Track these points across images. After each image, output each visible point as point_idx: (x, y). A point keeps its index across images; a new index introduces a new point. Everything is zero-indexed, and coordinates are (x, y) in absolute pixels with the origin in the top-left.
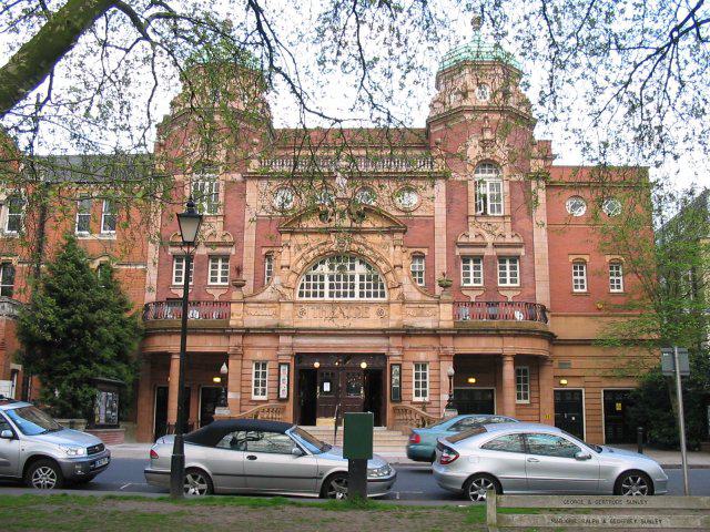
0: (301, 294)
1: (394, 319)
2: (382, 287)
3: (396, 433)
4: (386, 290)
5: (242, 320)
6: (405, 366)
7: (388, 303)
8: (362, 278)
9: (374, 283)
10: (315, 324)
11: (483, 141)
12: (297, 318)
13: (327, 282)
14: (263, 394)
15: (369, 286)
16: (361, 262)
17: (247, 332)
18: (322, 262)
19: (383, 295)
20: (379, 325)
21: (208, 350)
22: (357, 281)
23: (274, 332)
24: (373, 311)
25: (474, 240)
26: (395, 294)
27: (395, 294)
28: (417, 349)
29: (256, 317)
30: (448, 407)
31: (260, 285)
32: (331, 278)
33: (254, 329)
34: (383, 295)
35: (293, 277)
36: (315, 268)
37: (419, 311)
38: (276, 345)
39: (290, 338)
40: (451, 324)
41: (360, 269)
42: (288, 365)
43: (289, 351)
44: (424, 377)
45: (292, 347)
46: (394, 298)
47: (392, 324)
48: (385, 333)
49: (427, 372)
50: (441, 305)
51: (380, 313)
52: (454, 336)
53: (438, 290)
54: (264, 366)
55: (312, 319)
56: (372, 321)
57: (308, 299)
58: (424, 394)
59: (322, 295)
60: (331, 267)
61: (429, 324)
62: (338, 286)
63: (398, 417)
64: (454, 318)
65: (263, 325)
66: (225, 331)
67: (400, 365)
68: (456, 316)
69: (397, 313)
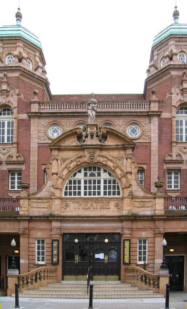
0: (66, 194)
1: (127, 209)
2: (118, 188)
3: (127, 285)
4: (121, 190)
5: (28, 211)
6: (133, 241)
7: (123, 199)
8: (105, 182)
9: (113, 186)
10: (75, 213)
11: (182, 90)
12: (63, 210)
13: (82, 185)
14: (43, 260)
15: (110, 187)
16: (105, 171)
17: (31, 219)
18: (80, 171)
19: (119, 194)
20: (116, 213)
21: (7, 231)
22: (102, 185)
23: (49, 218)
24: (112, 204)
25: (175, 159)
26: (127, 192)
27: (127, 192)
28: (140, 229)
29: (37, 209)
30: (162, 267)
31: (40, 185)
32: (85, 182)
33: (36, 217)
34: (119, 194)
35: (60, 180)
36: (75, 175)
37: (142, 204)
38: (50, 228)
39: (59, 223)
40: (163, 212)
41: (104, 176)
42: (58, 241)
43: (58, 232)
44: (145, 248)
45: (60, 228)
46: (126, 195)
47: (125, 213)
48: (121, 219)
49: (147, 245)
50: (157, 200)
51: (117, 206)
52: (164, 220)
53: (154, 189)
54: (43, 242)
55: (73, 210)
56: (112, 211)
57: (70, 196)
58: (144, 259)
59: (79, 193)
60: (86, 175)
61: (148, 212)
62: (90, 188)
63: (128, 275)
64: (165, 208)
65: (41, 214)
66: (16, 218)
67: (130, 240)
68: (166, 208)
69: (128, 206)
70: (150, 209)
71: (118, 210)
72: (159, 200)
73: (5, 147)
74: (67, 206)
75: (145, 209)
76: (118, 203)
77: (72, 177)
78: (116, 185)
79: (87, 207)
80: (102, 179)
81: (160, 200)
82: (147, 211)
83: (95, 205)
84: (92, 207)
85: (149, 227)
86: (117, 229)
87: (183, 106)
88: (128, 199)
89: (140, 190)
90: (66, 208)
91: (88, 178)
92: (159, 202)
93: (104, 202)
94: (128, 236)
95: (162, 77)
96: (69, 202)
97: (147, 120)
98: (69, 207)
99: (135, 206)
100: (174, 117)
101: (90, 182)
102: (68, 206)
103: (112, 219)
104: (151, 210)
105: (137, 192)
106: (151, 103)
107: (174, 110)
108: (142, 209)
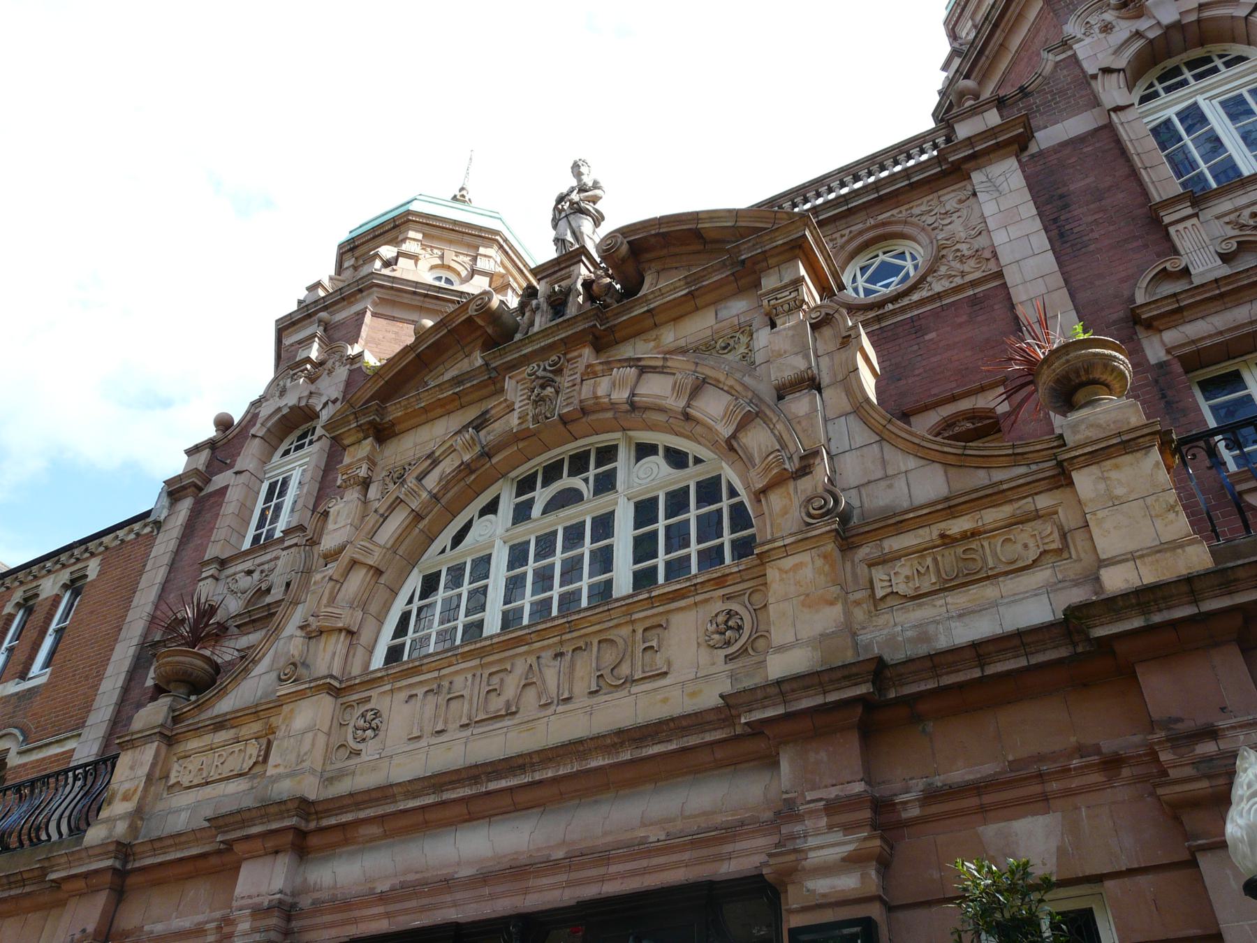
8: (645, 511)
32: (518, 556)
37: (948, 559)
60: (522, 513)
69: (810, 602)
70: (1041, 576)
71: (730, 666)
72: (1114, 475)
73: (258, 561)
74: (369, 733)
75: (989, 592)
76: (730, 614)
77: (443, 551)
78: (725, 504)
79: (497, 704)
80: (622, 501)
81: (1117, 467)
82: (1017, 598)
83: (551, 675)
84: (531, 695)
85: (1080, 751)
86: (731, 832)
87: (1170, 63)
88: (805, 557)
89: (912, 463)
90: (360, 746)
91: (539, 522)
92: (1119, 491)
93: (625, 631)
94: (848, 883)
95: (1003, 46)
96: (388, 699)
97: (950, 198)
98: (382, 734)
99: (880, 593)
100: (1118, 109)
101: (546, 545)
102: (376, 729)
103: (672, 746)
104: (1050, 589)
105: (883, 484)
106: (956, 126)
107: (1113, 92)
108: (958, 600)
